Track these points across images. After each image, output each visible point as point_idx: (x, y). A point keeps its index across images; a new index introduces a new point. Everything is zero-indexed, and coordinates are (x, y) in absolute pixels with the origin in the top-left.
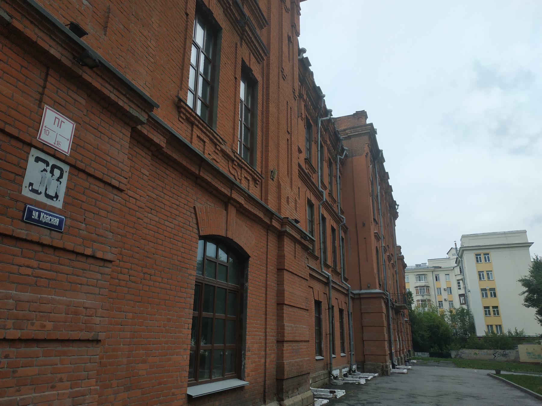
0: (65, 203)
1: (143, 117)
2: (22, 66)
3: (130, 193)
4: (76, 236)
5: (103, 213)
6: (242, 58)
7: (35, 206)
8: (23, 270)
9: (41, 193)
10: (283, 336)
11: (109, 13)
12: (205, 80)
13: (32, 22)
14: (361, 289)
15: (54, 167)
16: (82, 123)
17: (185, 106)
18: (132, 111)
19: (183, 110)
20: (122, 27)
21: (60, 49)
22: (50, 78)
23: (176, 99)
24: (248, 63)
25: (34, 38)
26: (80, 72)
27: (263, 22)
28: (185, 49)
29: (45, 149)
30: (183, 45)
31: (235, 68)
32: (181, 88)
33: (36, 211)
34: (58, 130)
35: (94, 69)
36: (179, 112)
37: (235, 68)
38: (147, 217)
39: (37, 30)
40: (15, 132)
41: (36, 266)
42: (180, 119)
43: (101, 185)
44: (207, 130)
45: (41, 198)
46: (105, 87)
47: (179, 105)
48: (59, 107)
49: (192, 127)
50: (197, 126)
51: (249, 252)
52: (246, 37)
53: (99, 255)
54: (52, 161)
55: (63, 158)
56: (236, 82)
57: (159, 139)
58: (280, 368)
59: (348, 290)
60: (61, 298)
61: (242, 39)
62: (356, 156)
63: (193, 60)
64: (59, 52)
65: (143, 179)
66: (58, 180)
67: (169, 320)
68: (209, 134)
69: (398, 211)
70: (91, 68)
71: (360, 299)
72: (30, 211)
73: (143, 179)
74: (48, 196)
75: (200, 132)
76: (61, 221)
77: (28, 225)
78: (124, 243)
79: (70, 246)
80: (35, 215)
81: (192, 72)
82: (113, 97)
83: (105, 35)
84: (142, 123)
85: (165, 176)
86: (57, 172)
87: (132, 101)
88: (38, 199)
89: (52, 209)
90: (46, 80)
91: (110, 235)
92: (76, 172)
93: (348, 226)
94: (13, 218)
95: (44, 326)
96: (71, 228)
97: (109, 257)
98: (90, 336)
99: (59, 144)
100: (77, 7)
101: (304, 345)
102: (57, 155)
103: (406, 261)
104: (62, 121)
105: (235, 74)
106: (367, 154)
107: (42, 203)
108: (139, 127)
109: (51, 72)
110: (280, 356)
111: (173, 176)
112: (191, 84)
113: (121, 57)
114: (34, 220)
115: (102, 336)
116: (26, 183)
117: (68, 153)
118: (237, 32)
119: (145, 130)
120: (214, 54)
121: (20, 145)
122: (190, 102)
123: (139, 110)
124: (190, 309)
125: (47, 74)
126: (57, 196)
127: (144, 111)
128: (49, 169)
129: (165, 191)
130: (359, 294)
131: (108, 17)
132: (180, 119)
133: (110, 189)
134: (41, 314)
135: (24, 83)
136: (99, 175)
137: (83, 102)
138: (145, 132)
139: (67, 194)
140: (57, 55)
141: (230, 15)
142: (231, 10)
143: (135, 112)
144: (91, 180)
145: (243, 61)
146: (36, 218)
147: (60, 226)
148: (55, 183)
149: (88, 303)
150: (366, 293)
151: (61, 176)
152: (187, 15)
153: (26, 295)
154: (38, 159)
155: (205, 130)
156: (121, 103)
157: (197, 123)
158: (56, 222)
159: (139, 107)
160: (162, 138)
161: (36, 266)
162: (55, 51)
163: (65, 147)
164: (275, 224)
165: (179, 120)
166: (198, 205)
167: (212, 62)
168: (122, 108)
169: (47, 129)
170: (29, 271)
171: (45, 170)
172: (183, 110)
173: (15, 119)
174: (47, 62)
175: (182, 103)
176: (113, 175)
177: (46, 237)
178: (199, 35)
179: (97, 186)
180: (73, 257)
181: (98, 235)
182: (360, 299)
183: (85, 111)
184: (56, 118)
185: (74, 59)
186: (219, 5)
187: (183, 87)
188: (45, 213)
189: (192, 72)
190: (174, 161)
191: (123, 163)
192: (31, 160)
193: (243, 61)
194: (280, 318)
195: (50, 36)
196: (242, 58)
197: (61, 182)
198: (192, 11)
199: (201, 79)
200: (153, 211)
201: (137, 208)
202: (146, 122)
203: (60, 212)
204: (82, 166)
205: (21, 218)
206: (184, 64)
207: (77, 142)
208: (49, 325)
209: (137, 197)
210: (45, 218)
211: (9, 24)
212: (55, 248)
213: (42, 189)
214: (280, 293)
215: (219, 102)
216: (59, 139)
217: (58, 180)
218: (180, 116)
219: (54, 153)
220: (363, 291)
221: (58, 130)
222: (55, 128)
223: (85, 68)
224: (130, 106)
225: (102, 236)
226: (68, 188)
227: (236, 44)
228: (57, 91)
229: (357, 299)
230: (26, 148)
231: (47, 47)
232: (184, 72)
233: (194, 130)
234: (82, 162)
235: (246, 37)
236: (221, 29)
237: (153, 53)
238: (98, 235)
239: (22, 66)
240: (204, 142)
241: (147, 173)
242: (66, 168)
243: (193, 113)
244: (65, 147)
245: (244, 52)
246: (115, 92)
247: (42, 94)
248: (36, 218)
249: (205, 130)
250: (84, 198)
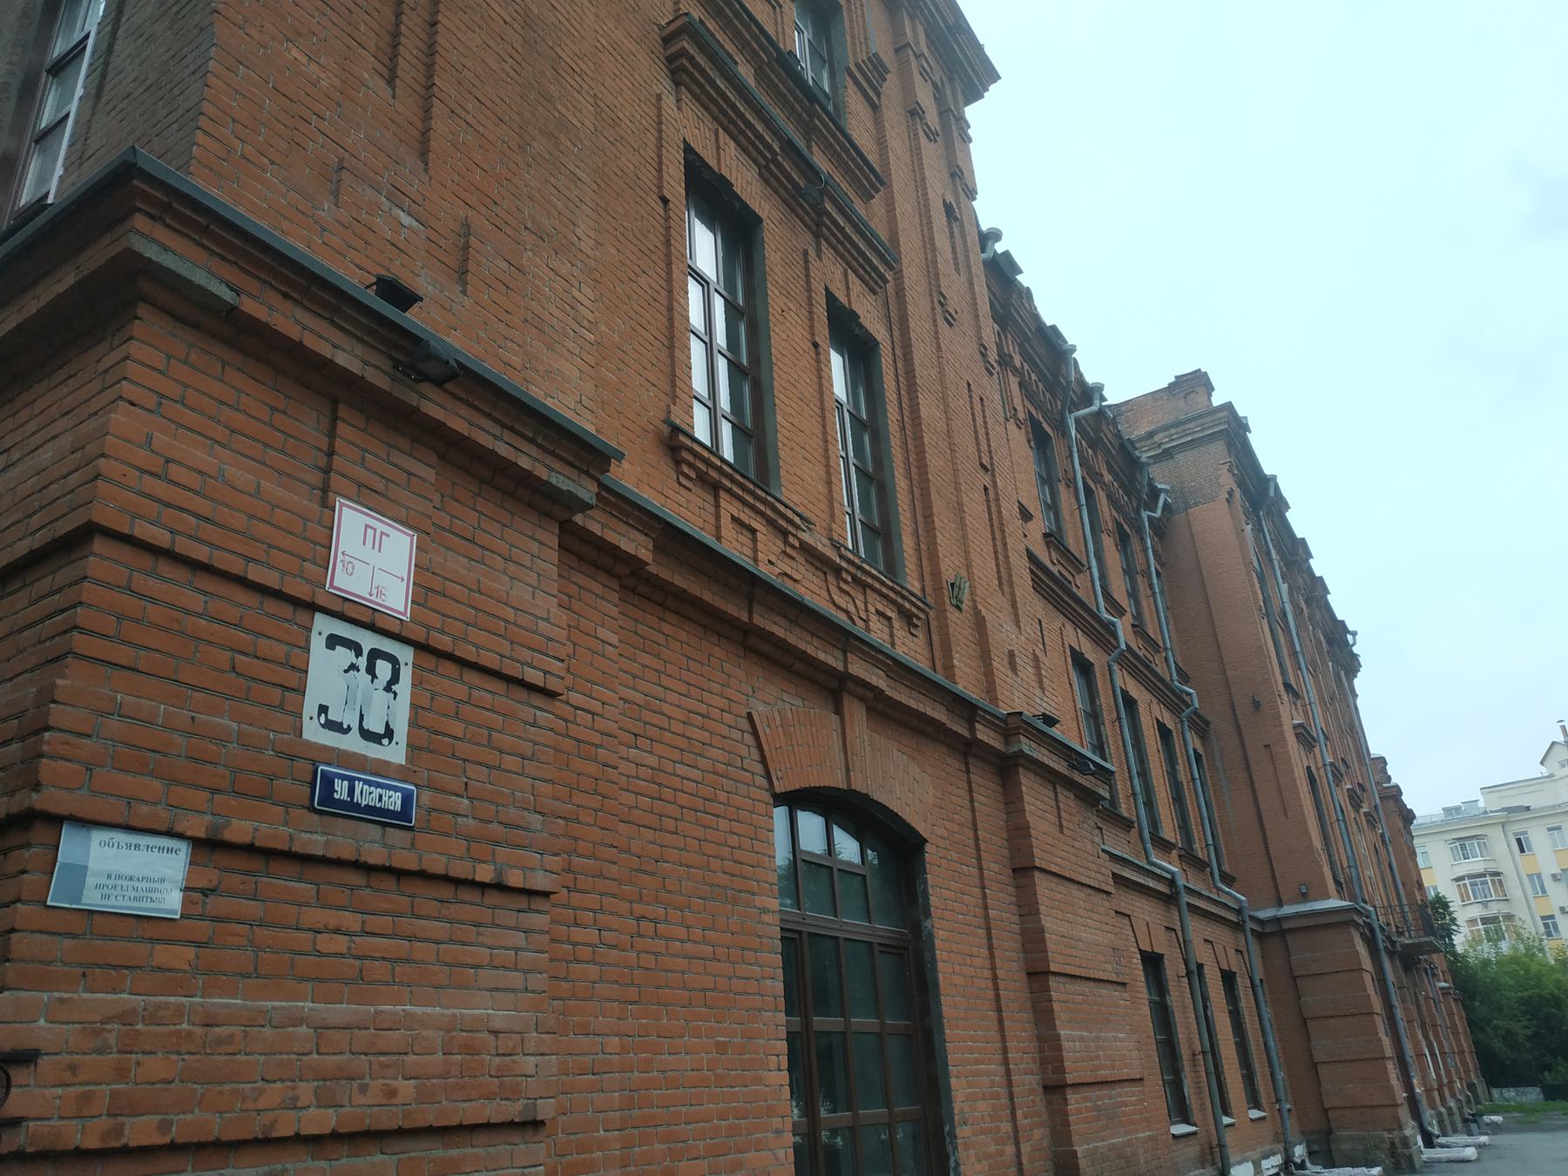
0: (412, 747)
1: (586, 491)
2: (274, 409)
3: (575, 697)
4: (448, 835)
5: (511, 762)
6: (827, 289)
7: (338, 766)
8: (326, 943)
9: (349, 728)
10: (1061, 1070)
11: (467, 235)
12: (734, 366)
13: (286, 296)
14: (1280, 904)
15: (375, 655)
16: (432, 530)
17: (689, 443)
18: (555, 480)
19: (686, 455)
20: (504, 265)
21: (358, 348)
22: (342, 428)
23: (666, 429)
24: (843, 299)
25: (294, 332)
26: (413, 400)
27: (871, 180)
28: (670, 291)
29: (349, 611)
30: (664, 284)
31: (811, 319)
32: (674, 398)
33: (343, 778)
34: (374, 558)
35: (448, 386)
36: (678, 462)
37: (811, 319)
38: (627, 759)
39: (300, 314)
40: (270, 579)
41: (357, 927)
42: (682, 480)
43: (500, 687)
44: (757, 497)
45: (352, 743)
46: (481, 428)
47: (675, 442)
48: (374, 499)
49: (716, 497)
50: (729, 491)
52: (828, 229)
53: (514, 879)
54: (369, 641)
55: (396, 629)
56: (818, 354)
57: (634, 544)
59: (1239, 912)
60: (429, 1010)
61: (817, 236)
62: (1196, 504)
63: (696, 318)
64: (356, 356)
65: (603, 656)
66: (388, 689)
67: (722, 1048)
68: (762, 507)
69: (1355, 650)
70: (439, 383)
71: (1282, 933)
72: (328, 781)
73: (603, 656)
74: (367, 735)
75: (740, 506)
76: (407, 800)
77: (325, 818)
78: (575, 839)
79: (436, 864)
80: (341, 790)
81: (697, 350)
82: (503, 450)
83: (464, 292)
84: (584, 507)
85: (661, 639)
86: (383, 669)
87: (552, 453)
88: (342, 747)
90: (332, 435)
91: (535, 820)
92: (430, 662)
93: (1209, 718)
94: (287, 805)
95: (393, 1093)
96: (434, 814)
97: (540, 881)
98: (513, 1110)
99: (380, 593)
100: (389, 235)
101: (1128, 1094)
102: (379, 624)
103: (1409, 800)
104: (382, 533)
105: (813, 335)
106: (1231, 493)
107: (353, 754)
108: (579, 519)
109: (343, 411)
111: (683, 636)
112: (699, 383)
113: (509, 344)
114: (340, 804)
115: (546, 1109)
116: (310, 708)
117: (404, 614)
118: (802, 220)
119: (595, 524)
120: (750, 292)
121: (286, 610)
122: (702, 432)
123: (573, 473)
124: (777, 1010)
125: (334, 420)
126: (389, 733)
127: (587, 473)
128: (362, 662)
129: (665, 680)
130: (1277, 920)
131: (467, 247)
132: (682, 480)
133: (523, 694)
134: (382, 1058)
135: (282, 452)
136: (489, 659)
137: (429, 474)
138: (596, 528)
139: (414, 723)
140: (355, 367)
141: (777, 179)
142: (779, 166)
143: (562, 479)
144: (472, 677)
145: (830, 297)
146: (345, 796)
147: (405, 813)
148: (382, 697)
149: (500, 1018)
150: (1299, 916)
151: (395, 679)
152: (665, 201)
153: (340, 1011)
154: (333, 641)
155: (749, 499)
156: (524, 463)
157: (727, 483)
158: (394, 801)
159: (571, 465)
160: (643, 537)
161: (357, 927)
162: (348, 356)
163: (396, 599)
164: (984, 734)
165: (680, 484)
166: (759, 709)
167: (747, 315)
168: (529, 474)
169: (348, 559)
170: (341, 943)
171: (353, 667)
172: (686, 455)
173: (270, 546)
174: (331, 389)
175: (682, 438)
176: (526, 655)
177: (373, 845)
178: (704, 248)
179: (489, 693)
180: (446, 892)
181: (506, 825)
182: (1282, 933)
183: (437, 497)
184: (367, 526)
185: (395, 367)
186: (744, 158)
187: (679, 393)
188: (366, 782)
189: (697, 350)
190: (682, 596)
191: (547, 620)
192: (317, 643)
193: (830, 297)
194: (1043, 1015)
195: (333, 323)
196: (827, 289)
197: (395, 694)
198: (675, 186)
199: (722, 365)
200: (640, 741)
201: (597, 738)
202: (594, 501)
203: (402, 773)
204: (443, 642)
205: (307, 803)
206: (673, 333)
207: (426, 583)
208: (406, 1088)
209: (596, 706)
210: (367, 795)
211: (233, 309)
212: (399, 874)
213: (351, 720)
214: (1033, 940)
215: (779, 418)
216: (381, 580)
217: (388, 689)
218: (680, 473)
219: (370, 619)
220: (1288, 910)
221: (374, 558)
222: (367, 553)
223: (427, 388)
224: (548, 467)
225: (517, 827)
226: (415, 707)
227: (806, 253)
228: (363, 458)
229: (1271, 934)
230: (301, 616)
231: (326, 350)
232: (677, 353)
233: (723, 503)
234: (443, 633)
235: (828, 229)
236: (760, 220)
237: (591, 317)
238: (506, 825)
239: (274, 409)
240: (753, 531)
241: (614, 639)
242: (405, 654)
243: (713, 459)
244: (396, 599)
245: (830, 272)
246: (507, 435)
247: (327, 471)
248: (345, 796)
249: (749, 499)
250: (458, 728)
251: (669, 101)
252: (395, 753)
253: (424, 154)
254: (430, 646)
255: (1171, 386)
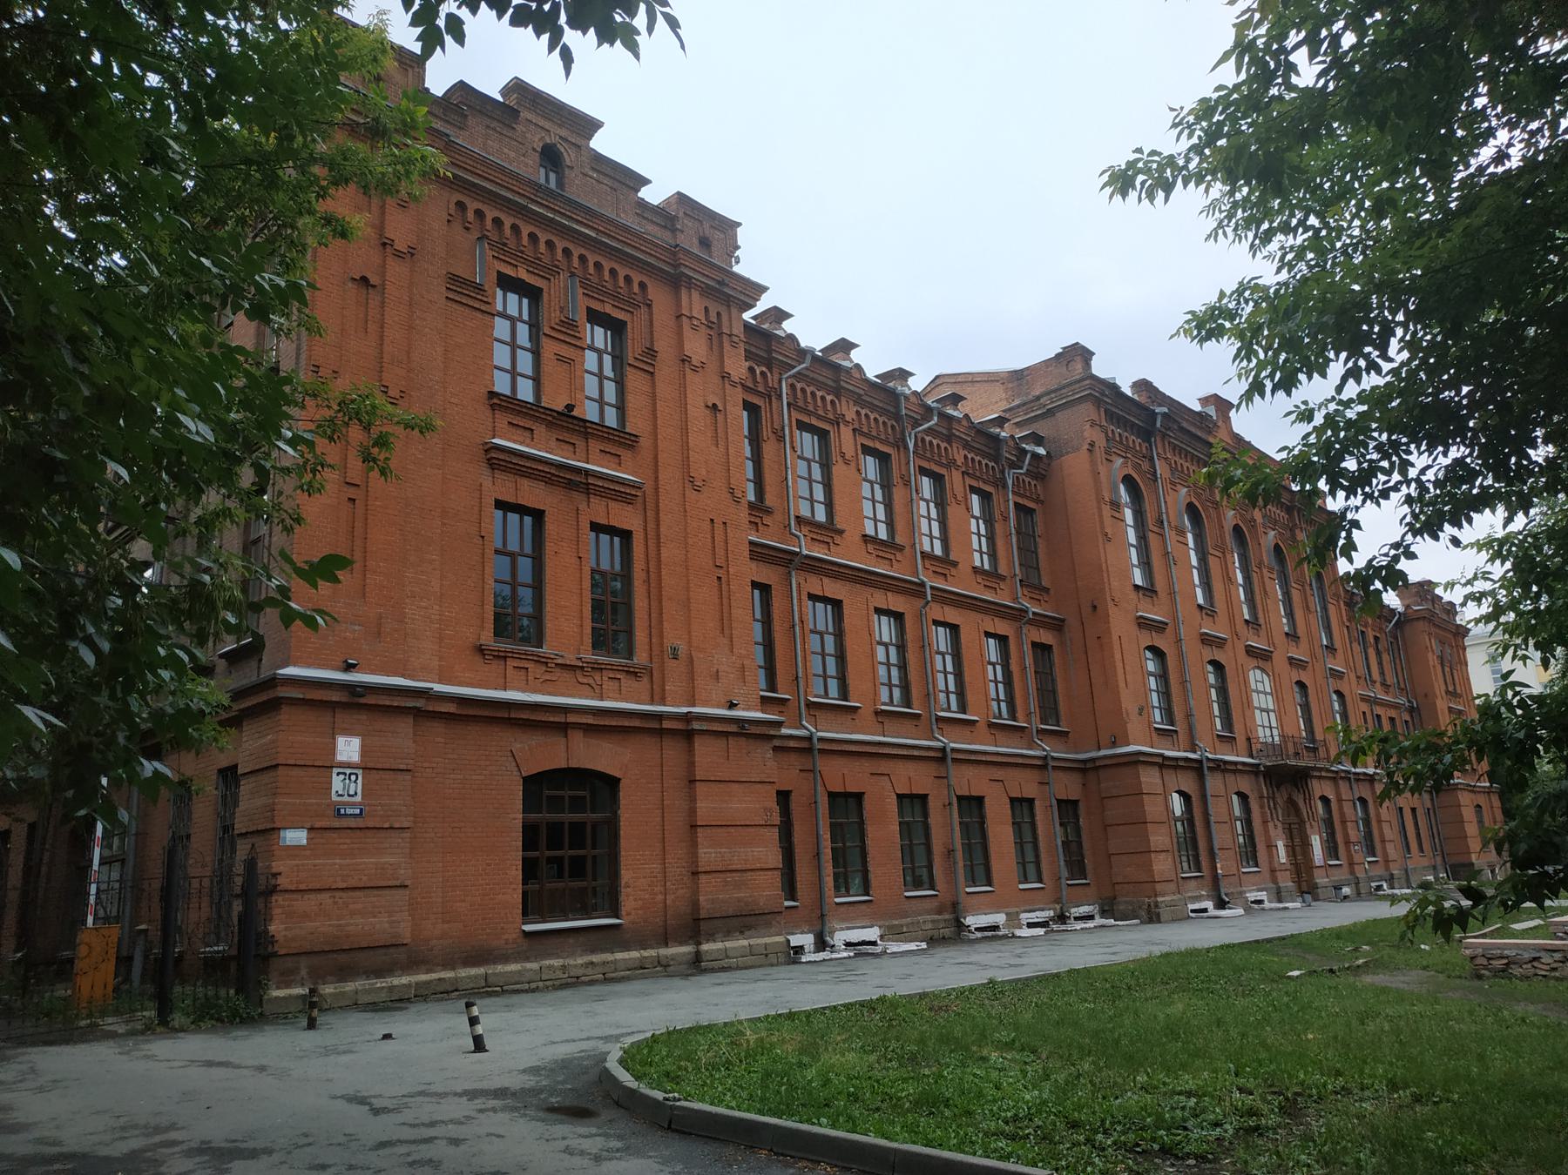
45: (346, 798)
51: (617, 774)
54: (348, 771)
58: (695, 905)
79: (371, 824)
82: (388, 703)
89: (353, 805)
98: (398, 883)
101: (762, 878)
106: (1092, 444)
110: (696, 892)
115: (408, 883)
130: (1093, 760)
149: (392, 860)
150: (1105, 757)
163: (355, 757)
164: (666, 724)
177: (352, 823)
207: (364, 751)
210: (349, 811)
214: (692, 811)
220: (1103, 753)
221: (348, 748)
244: (355, 757)
251: (487, 482)
252: (358, 798)
253: (364, 596)
254: (366, 767)
255: (1058, 356)
